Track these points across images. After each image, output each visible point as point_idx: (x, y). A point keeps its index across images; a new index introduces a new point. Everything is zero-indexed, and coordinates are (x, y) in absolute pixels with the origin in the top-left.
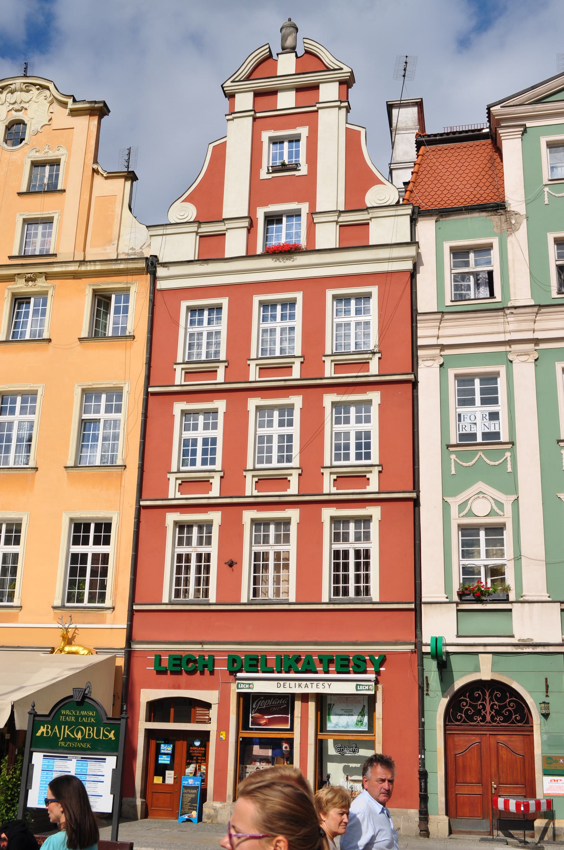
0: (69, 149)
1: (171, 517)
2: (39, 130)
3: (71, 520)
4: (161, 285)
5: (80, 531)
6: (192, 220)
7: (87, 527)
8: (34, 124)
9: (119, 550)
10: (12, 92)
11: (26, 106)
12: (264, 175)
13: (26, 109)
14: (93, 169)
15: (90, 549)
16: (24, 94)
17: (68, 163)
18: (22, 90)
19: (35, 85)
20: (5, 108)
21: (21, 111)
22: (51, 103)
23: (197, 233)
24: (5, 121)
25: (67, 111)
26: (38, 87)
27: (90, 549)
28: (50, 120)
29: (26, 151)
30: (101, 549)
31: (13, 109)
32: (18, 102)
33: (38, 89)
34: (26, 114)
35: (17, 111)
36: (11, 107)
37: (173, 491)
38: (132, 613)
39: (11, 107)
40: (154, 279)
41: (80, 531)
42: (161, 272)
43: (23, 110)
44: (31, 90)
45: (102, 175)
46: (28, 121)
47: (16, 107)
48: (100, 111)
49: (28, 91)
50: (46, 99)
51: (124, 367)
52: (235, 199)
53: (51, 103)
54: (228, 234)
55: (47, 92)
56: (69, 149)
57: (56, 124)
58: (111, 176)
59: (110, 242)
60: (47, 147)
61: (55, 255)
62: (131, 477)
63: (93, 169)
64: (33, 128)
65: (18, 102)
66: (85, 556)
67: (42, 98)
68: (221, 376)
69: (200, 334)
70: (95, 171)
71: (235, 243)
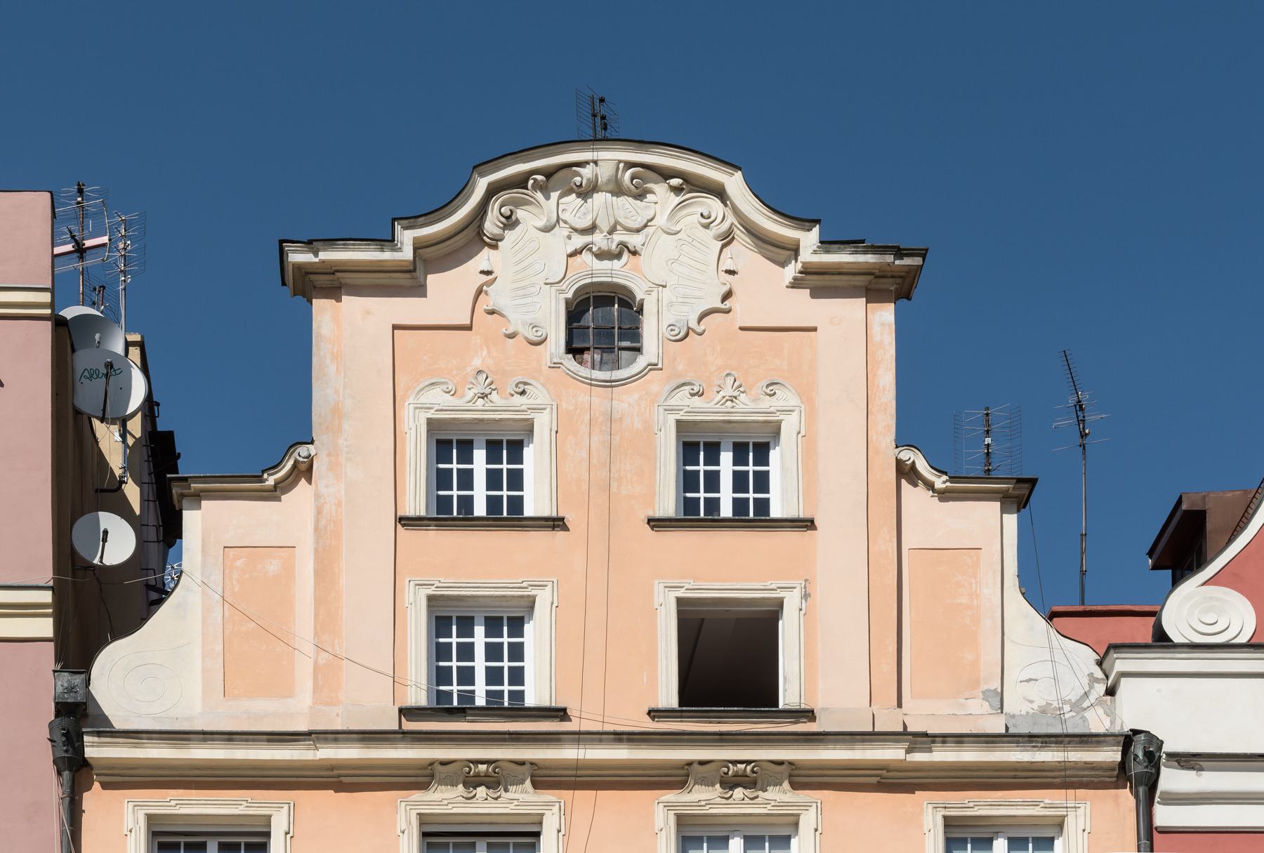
0: (807, 395)
2: (693, 324)
6: (1243, 639)
8: (671, 304)
11: (634, 240)
13: (634, 253)
14: (899, 463)
16: (625, 202)
18: (618, 191)
19: (665, 174)
20: (561, 244)
21: (618, 256)
22: (727, 239)
24: (564, 286)
25: (791, 270)
26: (676, 182)
28: (727, 295)
29: (655, 388)
31: (586, 247)
32: (604, 225)
33: (677, 190)
34: (636, 268)
35: (602, 255)
36: (579, 241)
39: (579, 241)
43: (626, 255)
44: (652, 192)
45: (930, 486)
46: (649, 292)
47: (599, 240)
49: (640, 195)
50: (707, 226)
53: (727, 239)
55: (713, 205)
56: (807, 395)
60: (730, 380)
63: (899, 463)
64: (668, 318)
65: (604, 225)
67: (690, 218)
70: (906, 472)
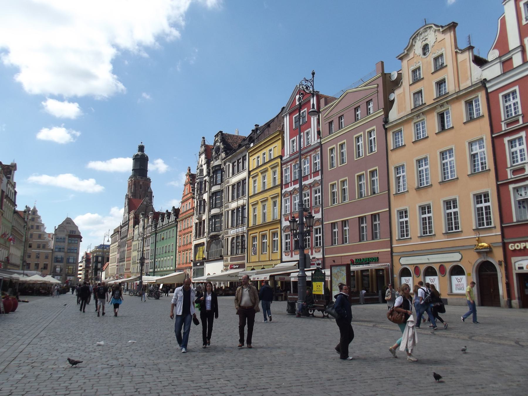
1: (511, 187)
3: (474, 195)
4: (489, 90)
5: (478, 198)
7: (481, 196)
9: (493, 203)
10: (421, 34)
12: (524, 22)
15: (483, 205)
17: (445, 53)
23: (500, 62)
27: (483, 205)
30: (487, 204)
37: (510, 175)
38: (502, 228)
40: (486, 89)
41: (478, 198)
42: (488, 85)
48: (453, 26)
51: (482, 129)
52: (513, 41)
54: (514, 57)
57: (438, 40)
58: (463, 51)
59: (468, 79)
61: (448, 93)
62: (492, 173)
66: (482, 208)
68: (521, 122)
69: (510, 105)
71: (517, 60)
